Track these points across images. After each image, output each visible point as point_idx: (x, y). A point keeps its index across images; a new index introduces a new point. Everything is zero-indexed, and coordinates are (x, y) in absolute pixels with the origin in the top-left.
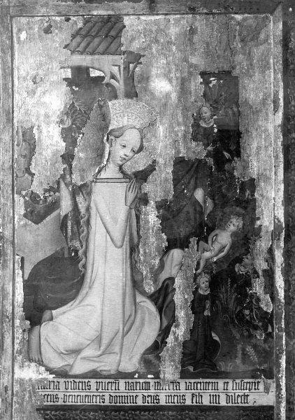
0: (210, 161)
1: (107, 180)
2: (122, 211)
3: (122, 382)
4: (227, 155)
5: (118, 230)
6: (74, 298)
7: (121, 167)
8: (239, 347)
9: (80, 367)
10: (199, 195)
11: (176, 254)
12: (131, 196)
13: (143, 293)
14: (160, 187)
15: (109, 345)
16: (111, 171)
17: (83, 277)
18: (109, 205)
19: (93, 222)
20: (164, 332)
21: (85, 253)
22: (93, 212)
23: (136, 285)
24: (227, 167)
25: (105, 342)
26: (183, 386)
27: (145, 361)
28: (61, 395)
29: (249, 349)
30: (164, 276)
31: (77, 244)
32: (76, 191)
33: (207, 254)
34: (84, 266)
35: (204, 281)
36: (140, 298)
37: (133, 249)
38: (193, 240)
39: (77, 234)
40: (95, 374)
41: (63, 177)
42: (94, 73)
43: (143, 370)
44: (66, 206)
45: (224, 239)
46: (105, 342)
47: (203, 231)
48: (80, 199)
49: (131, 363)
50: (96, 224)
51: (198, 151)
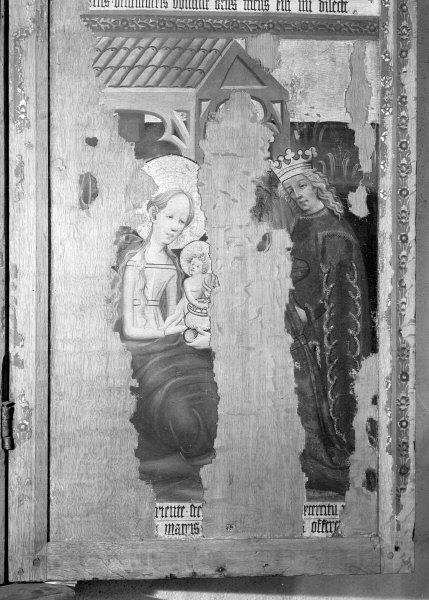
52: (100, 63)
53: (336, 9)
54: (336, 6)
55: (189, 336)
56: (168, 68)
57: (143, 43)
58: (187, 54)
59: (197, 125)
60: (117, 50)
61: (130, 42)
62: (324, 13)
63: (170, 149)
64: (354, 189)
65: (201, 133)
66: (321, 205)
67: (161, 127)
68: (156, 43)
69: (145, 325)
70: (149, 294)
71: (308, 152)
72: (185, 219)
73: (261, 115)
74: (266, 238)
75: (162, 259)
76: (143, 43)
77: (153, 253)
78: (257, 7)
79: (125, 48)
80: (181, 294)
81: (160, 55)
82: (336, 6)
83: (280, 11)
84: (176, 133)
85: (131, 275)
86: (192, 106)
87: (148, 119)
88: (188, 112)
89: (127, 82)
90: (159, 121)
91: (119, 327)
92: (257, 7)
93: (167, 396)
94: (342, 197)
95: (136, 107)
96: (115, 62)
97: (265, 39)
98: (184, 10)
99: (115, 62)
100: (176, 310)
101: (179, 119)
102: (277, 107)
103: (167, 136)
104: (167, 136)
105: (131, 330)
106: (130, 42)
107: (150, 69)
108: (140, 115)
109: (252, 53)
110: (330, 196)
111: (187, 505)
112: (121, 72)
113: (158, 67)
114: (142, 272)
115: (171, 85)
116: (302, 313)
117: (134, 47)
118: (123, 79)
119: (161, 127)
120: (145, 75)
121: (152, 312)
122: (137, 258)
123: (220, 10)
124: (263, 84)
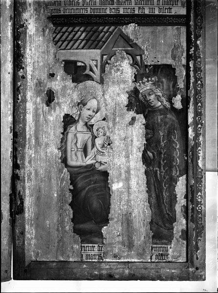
28: (62, 9)
52: (56, 39)
53: (166, 12)
54: (166, 10)
55: (97, 165)
56: (88, 41)
58: (97, 34)
59: (101, 66)
60: (64, 33)
62: (161, 13)
63: (89, 77)
64: (175, 96)
65: (103, 70)
66: (160, 104)
67: (85, 68)
68: (82, 29)
69: (77, 160)
70: (79, 145)
71: (153, 79)
72: (95, 110)
74: (133, 119)
75: (85, 129)
77: (80, 126)
78: (129, 12)
79: (68, 32)
80: (93, 145)
81: (84, 35)
82: (166, 10)
83: (140, 13)
84: (91, 70)
85: (70, 136)
86: (99, 58)
87: (79, 64)
88: (97, 60)
89: (69, 47)
90: (83, 64)
91: (64, 160)
92: (129, 12)
93: (88, 192)
94: (170, 100)
96: (64, 37)
98: (95, 13)
99: (64, 37)
100: (91, 153)
101: (93, 63)
102: (138, 58)
103: (87, 72)
104: (87, 72)
105: (72, 162)
106: (70, 29)
107: (79, 41)
108: (75, 62)
110: (164, 99)
111: (96, 245)
112: (66, 43)
113: (83, 40)
114: (75, 135)
115: (89, 48)
116: (151, 155)
117: (72, 31)
118: (67, 46)
119: (85, 68)
120: (77, 44)
121: (79, 154)
122: (73, 128)
123: (112, 13)
124: (132, 47)
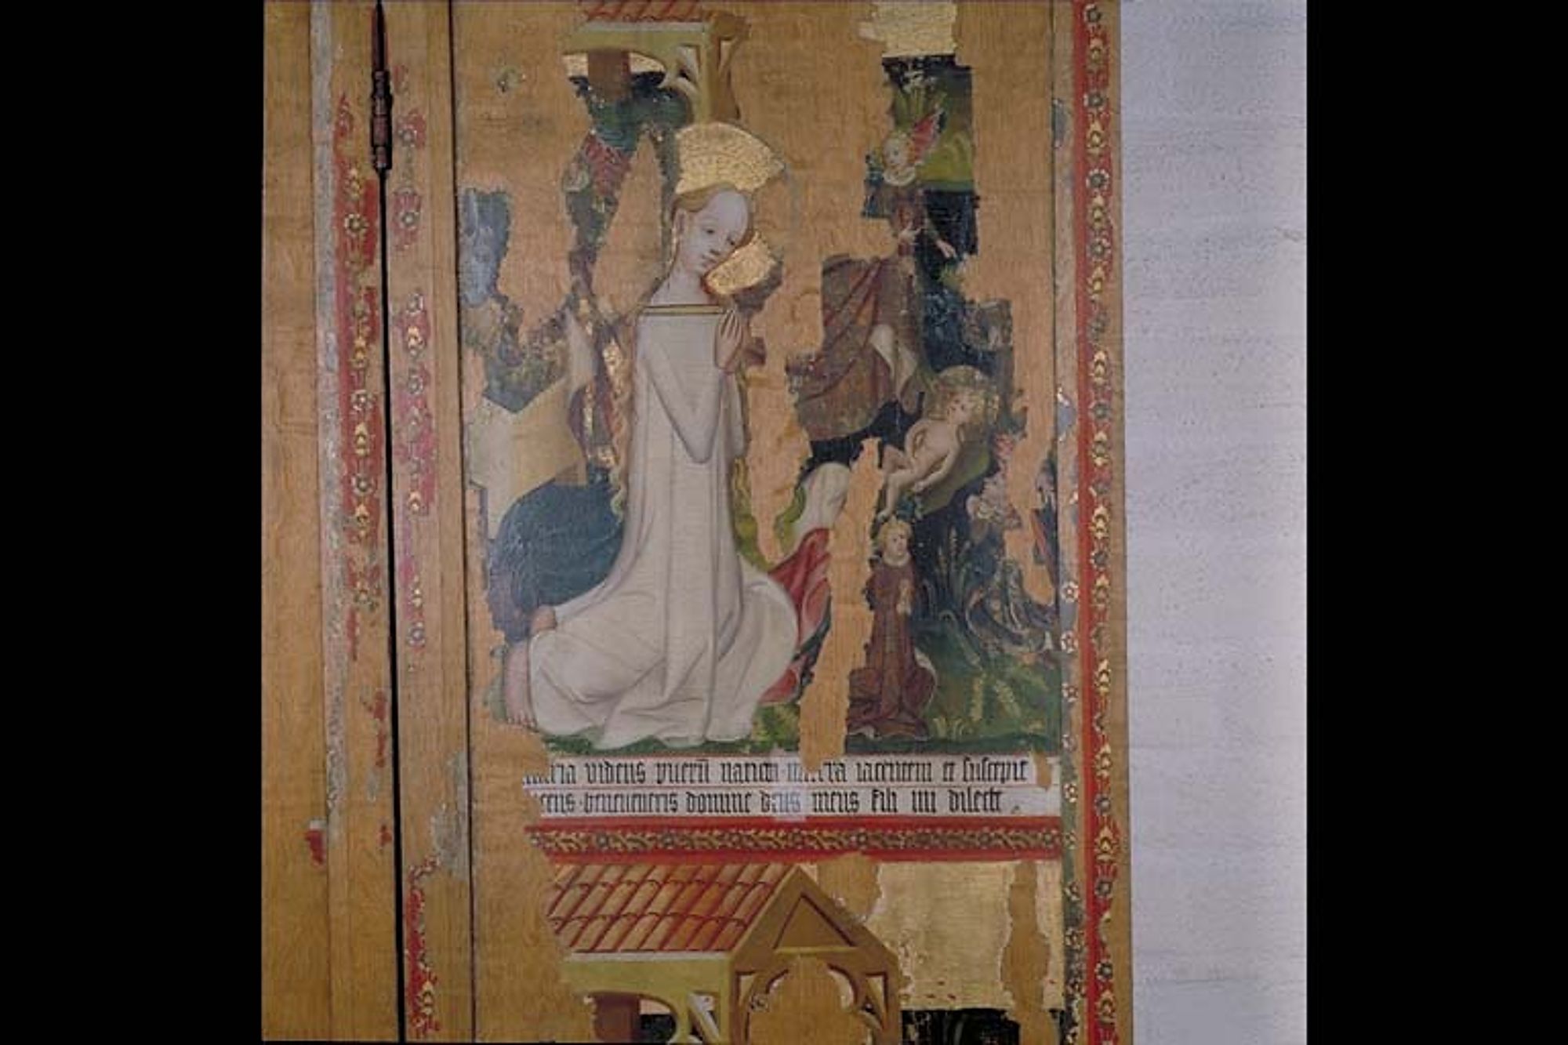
0: (909, 266)
1: (672, 310)
2: (708, 377)
3: (715, 763)
4: (947, 249)
5: (698, 424)
6: (603, 576)
7: (703, 282)
8: (978, 685)
9: (618, 736)
10: (883, 340)
11: (831, 470)
12: (728, 345)
13: (758, 562)
14: (796, 329)
15: (685, 681)
16: (681, 289)
17: (620, 533)
18: (676, 364)
19: (641, 405)
20: (809, 651)
21: (625, 475)
22: (642, 379)
23: (744, 543)
24: (946, 273)
25: (674, 674)
26: (851, 773)
27: (767, 718)
28: (578, 797)
29: (1003, 690)
30: (805, 524)
31: (606, 457)
32: (603, 334)
33: (902, 476)
34: (624, 505)
35: (897, 534)
36: (751, 574)
37: (735, 467)
38: (870, 444)
39: (604, 435)
40: (649, 747)
41: (572, 304)
42: (641, 66)
43: (761, 737)
44: (581, 371)
45: (937, 442)
46: (674, 674)
47: (892, 425)
48: (612, 353)
49: (738, 723)
50: (647, 405)
51: (877, 241)
52: (560, 912)
56: (681, 917)
57: (634, 875)
61: (658, 873)
73: (847, 993)
76: (634, 875)
81: (665, 895)
86: (723, 984)
87: (648, 1008)
89: (608, 941)
95: (625, 988)
97: (850, 864)
101: (703, 1006)
108: (633, 1001)
109: (829, 890)
115: (685, 947)
